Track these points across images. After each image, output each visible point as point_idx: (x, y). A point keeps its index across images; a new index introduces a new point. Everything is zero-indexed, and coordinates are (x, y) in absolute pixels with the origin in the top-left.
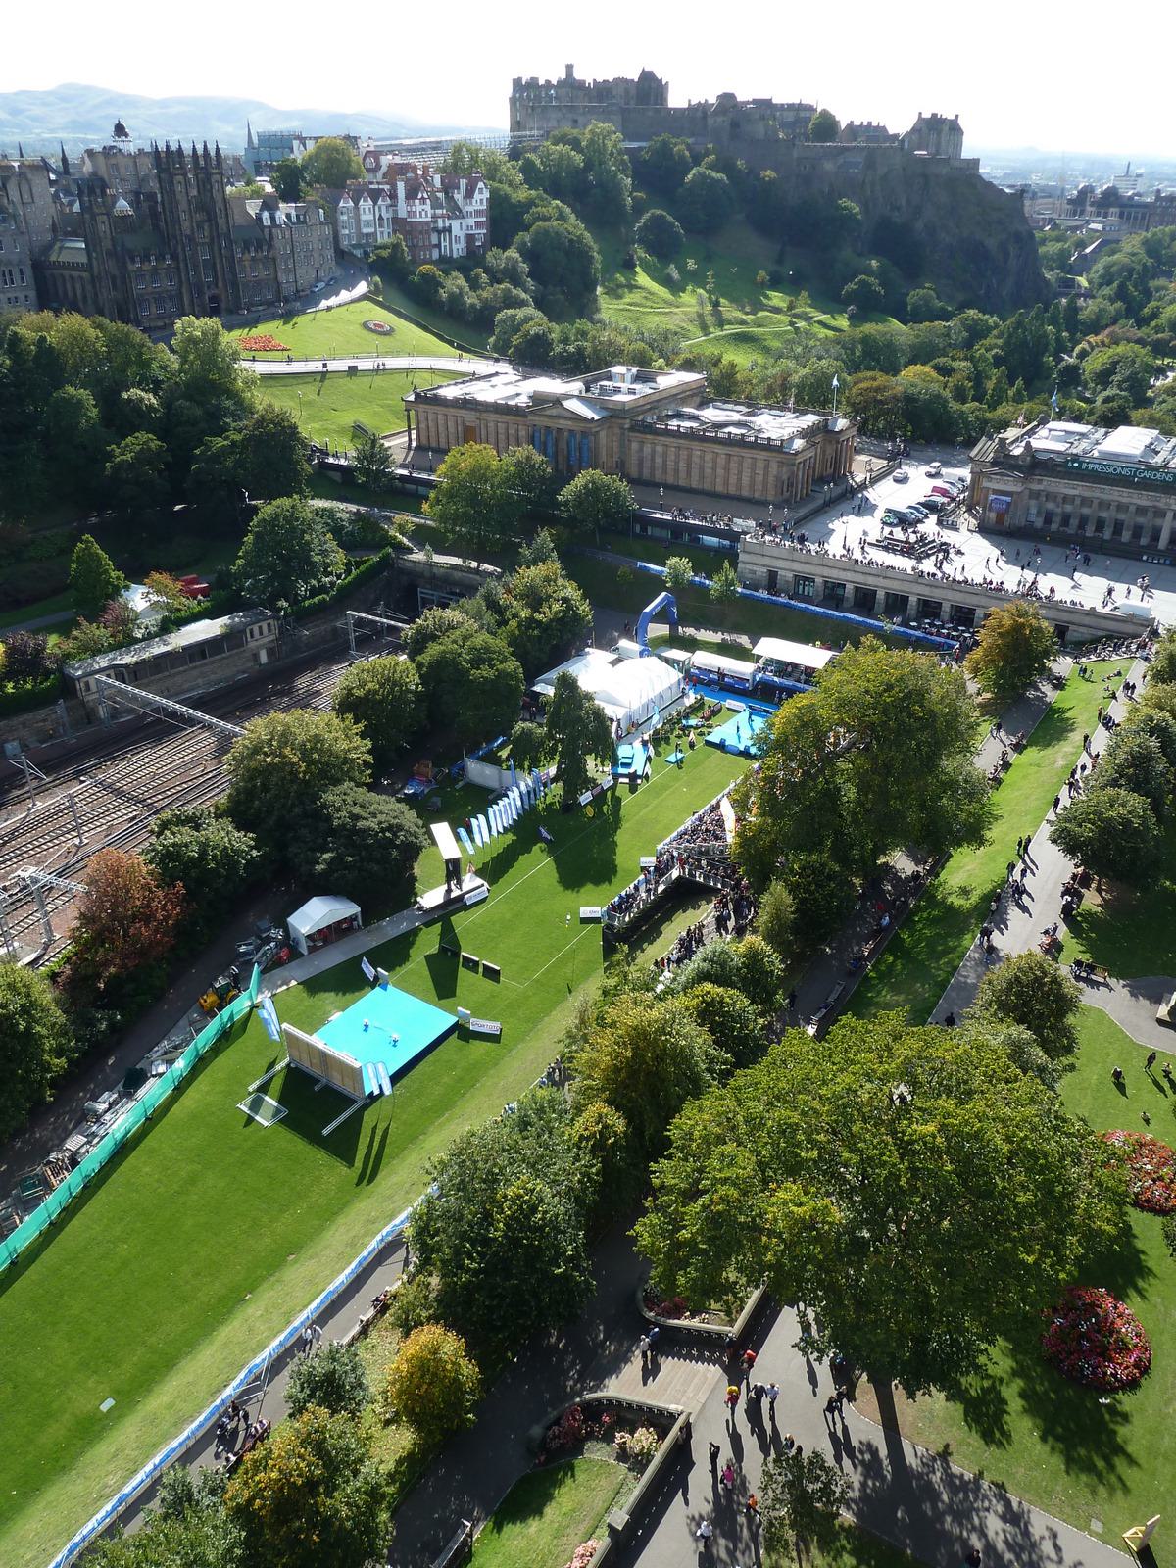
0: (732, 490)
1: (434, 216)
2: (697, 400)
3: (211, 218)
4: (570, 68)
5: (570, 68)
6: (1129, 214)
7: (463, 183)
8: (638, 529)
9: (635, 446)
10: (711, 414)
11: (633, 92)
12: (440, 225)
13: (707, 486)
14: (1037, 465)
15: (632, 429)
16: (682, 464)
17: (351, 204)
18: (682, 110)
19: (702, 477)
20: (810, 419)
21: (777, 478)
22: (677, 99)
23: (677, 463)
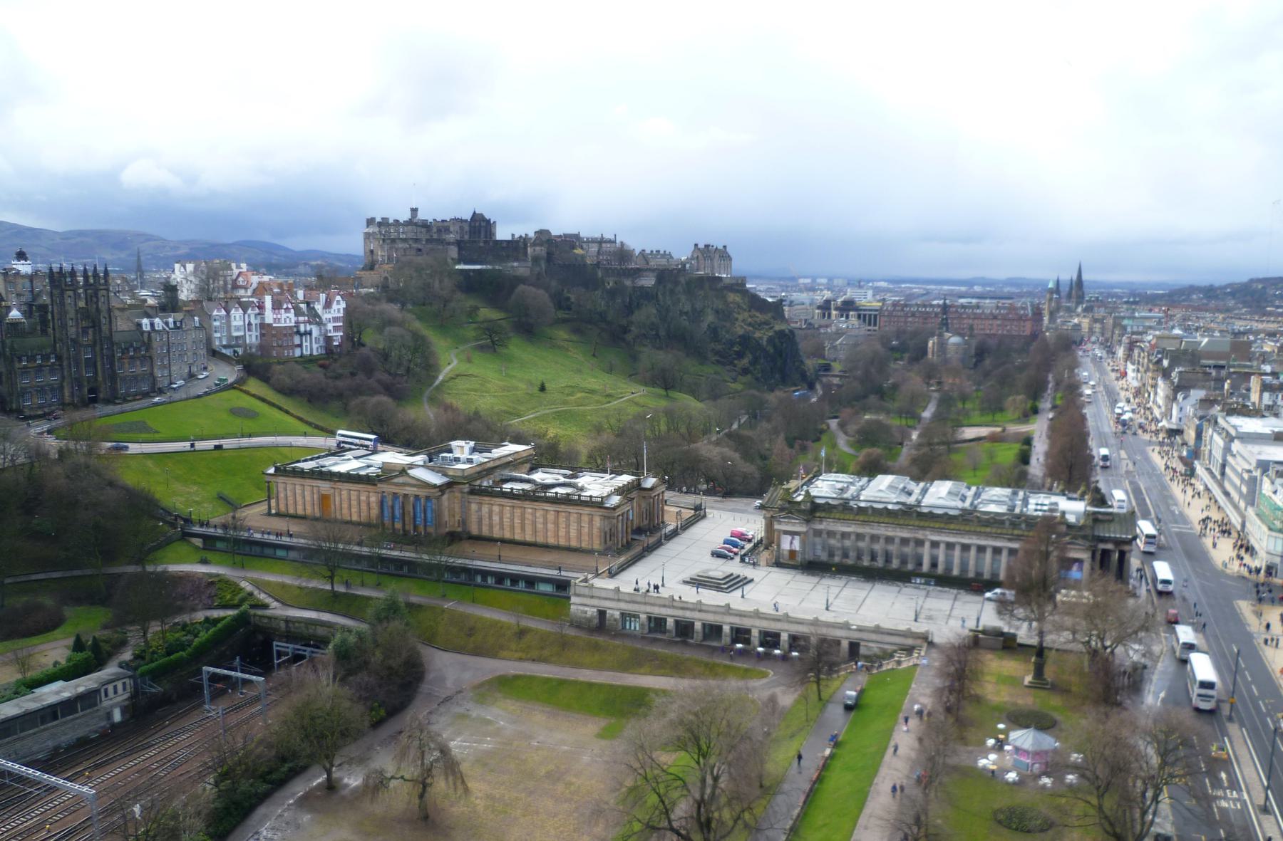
0: (562, 542)
1: (297, 323)
2: (528, 466)
3: (96, 325)
4: (414, 211)
5: (414, 211)
7: (323, 297)
8: (479, 579)
9: (474, 507)
10: (539, 476)
11: (467, 228)
12: (302, 329)
13: (540, 539)
14: (815, 510)
16: (517, 521)
17: (223, 312)
18: (508, 242)
19: (535, 531)
20: (626, 479)
22: (502, 233)
23: (512, 520)
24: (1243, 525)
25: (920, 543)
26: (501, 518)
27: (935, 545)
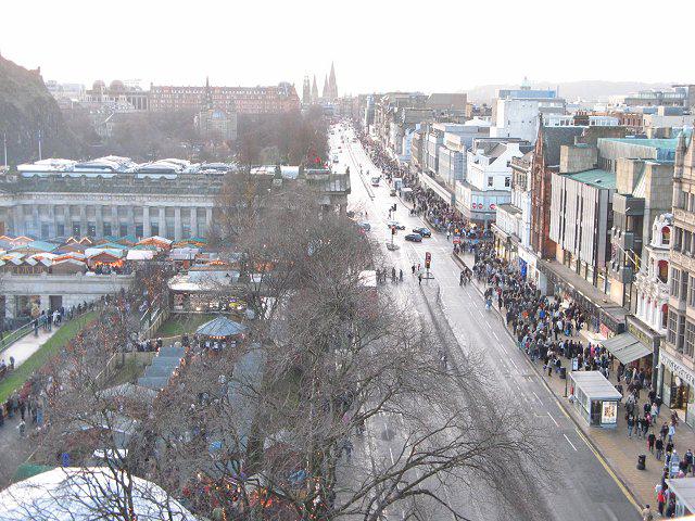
6: (134, 99)
24: (453, 199)
25: (137, 210)
27: (153, 211)
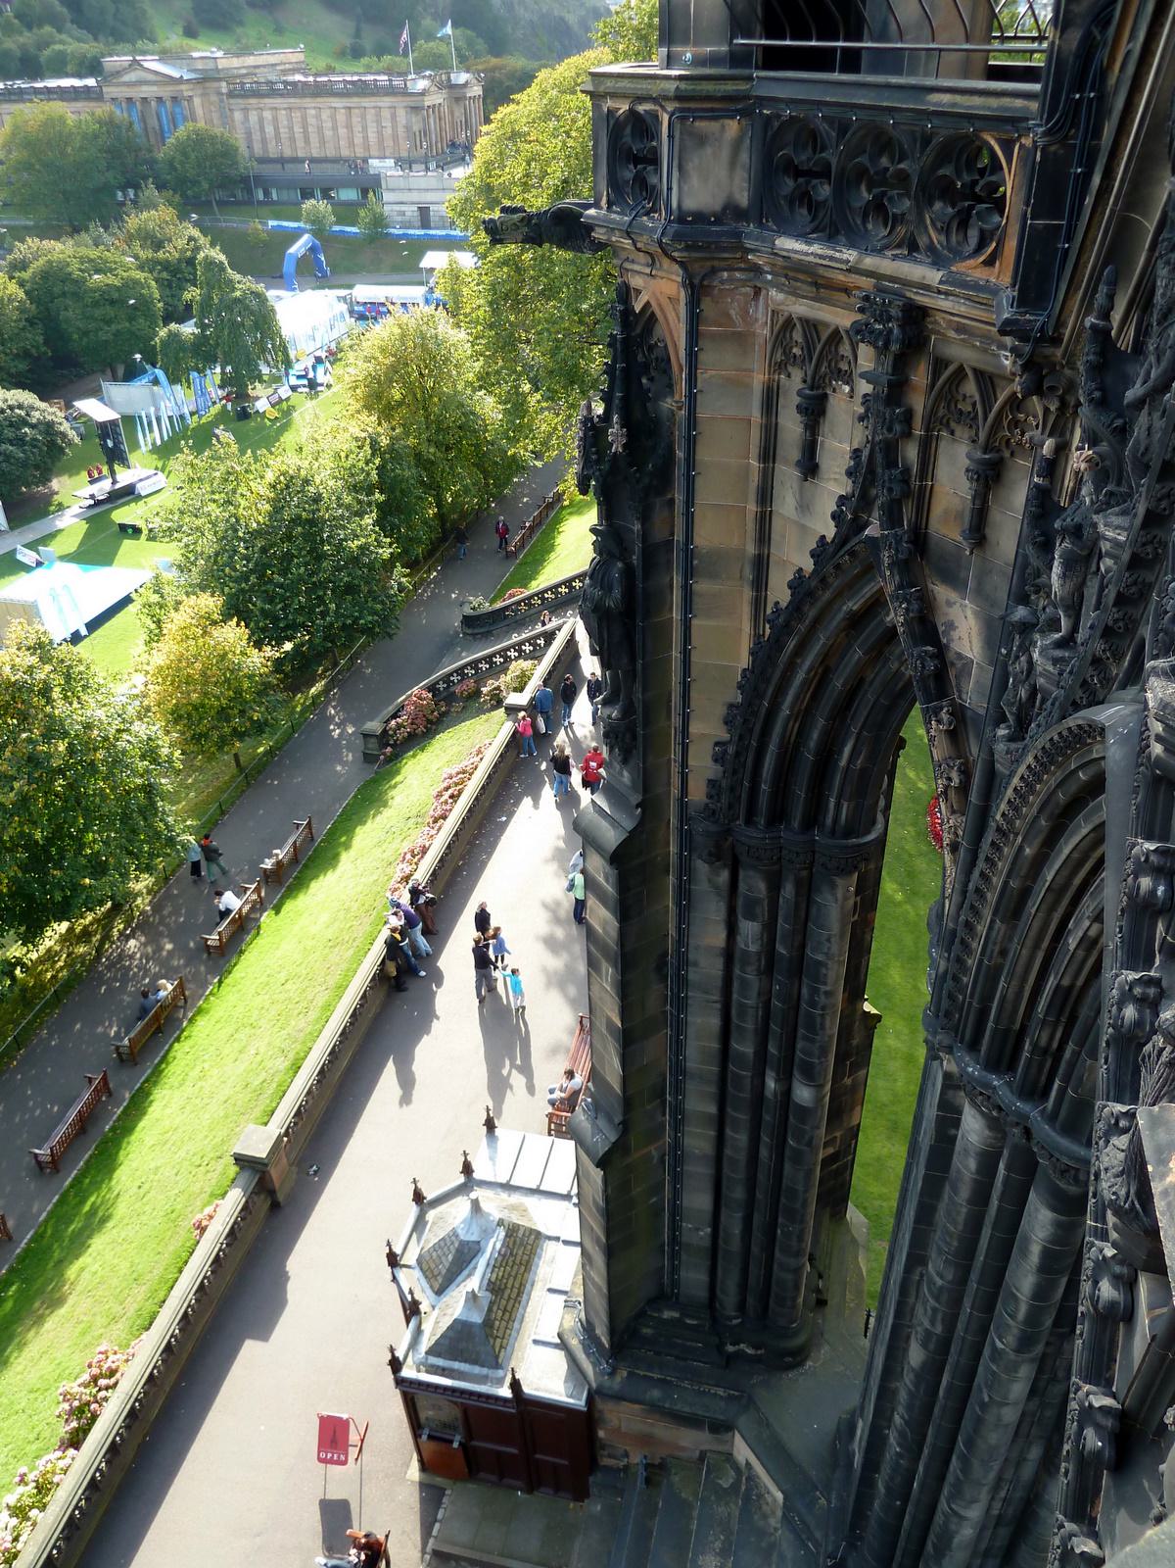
9: (238, 116)
15: (231, 95)
16: (297, 129)
19: (323, 142)
21: (408, 128)
26: (276, 129)
